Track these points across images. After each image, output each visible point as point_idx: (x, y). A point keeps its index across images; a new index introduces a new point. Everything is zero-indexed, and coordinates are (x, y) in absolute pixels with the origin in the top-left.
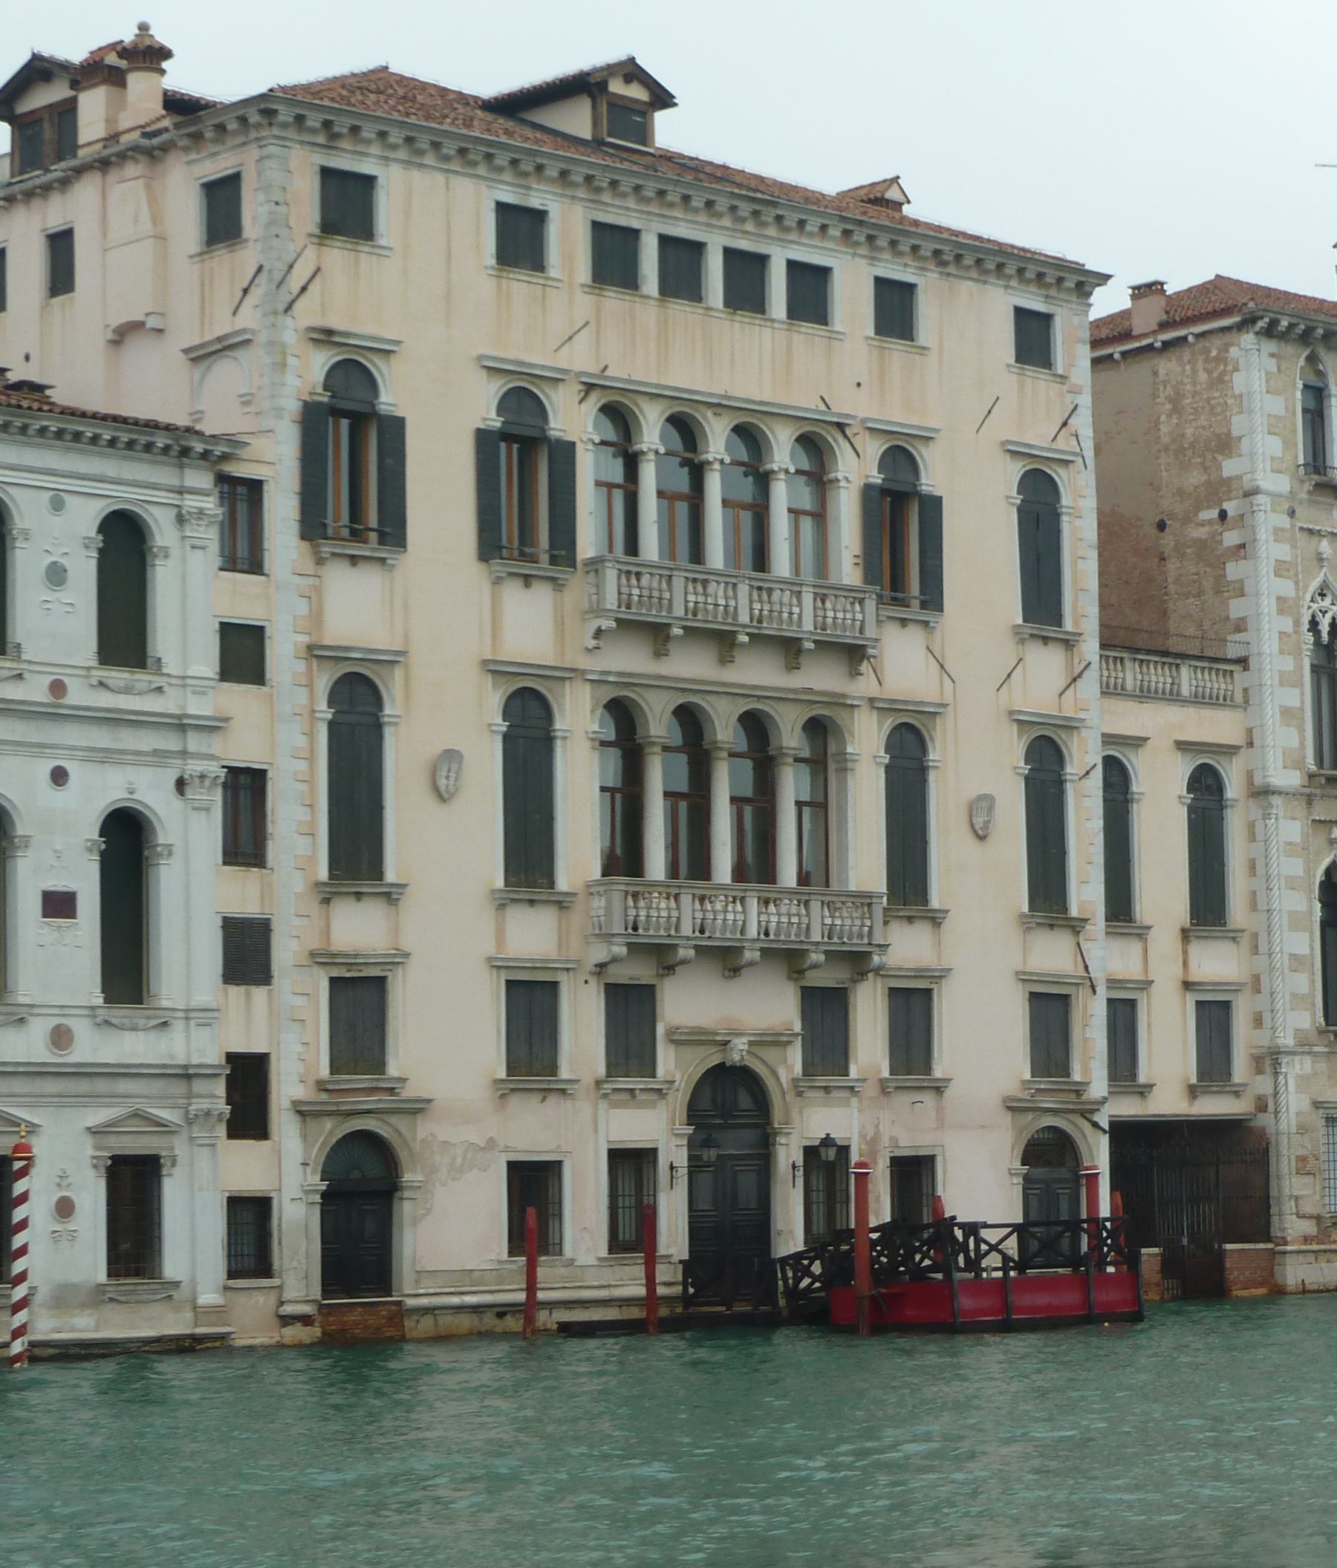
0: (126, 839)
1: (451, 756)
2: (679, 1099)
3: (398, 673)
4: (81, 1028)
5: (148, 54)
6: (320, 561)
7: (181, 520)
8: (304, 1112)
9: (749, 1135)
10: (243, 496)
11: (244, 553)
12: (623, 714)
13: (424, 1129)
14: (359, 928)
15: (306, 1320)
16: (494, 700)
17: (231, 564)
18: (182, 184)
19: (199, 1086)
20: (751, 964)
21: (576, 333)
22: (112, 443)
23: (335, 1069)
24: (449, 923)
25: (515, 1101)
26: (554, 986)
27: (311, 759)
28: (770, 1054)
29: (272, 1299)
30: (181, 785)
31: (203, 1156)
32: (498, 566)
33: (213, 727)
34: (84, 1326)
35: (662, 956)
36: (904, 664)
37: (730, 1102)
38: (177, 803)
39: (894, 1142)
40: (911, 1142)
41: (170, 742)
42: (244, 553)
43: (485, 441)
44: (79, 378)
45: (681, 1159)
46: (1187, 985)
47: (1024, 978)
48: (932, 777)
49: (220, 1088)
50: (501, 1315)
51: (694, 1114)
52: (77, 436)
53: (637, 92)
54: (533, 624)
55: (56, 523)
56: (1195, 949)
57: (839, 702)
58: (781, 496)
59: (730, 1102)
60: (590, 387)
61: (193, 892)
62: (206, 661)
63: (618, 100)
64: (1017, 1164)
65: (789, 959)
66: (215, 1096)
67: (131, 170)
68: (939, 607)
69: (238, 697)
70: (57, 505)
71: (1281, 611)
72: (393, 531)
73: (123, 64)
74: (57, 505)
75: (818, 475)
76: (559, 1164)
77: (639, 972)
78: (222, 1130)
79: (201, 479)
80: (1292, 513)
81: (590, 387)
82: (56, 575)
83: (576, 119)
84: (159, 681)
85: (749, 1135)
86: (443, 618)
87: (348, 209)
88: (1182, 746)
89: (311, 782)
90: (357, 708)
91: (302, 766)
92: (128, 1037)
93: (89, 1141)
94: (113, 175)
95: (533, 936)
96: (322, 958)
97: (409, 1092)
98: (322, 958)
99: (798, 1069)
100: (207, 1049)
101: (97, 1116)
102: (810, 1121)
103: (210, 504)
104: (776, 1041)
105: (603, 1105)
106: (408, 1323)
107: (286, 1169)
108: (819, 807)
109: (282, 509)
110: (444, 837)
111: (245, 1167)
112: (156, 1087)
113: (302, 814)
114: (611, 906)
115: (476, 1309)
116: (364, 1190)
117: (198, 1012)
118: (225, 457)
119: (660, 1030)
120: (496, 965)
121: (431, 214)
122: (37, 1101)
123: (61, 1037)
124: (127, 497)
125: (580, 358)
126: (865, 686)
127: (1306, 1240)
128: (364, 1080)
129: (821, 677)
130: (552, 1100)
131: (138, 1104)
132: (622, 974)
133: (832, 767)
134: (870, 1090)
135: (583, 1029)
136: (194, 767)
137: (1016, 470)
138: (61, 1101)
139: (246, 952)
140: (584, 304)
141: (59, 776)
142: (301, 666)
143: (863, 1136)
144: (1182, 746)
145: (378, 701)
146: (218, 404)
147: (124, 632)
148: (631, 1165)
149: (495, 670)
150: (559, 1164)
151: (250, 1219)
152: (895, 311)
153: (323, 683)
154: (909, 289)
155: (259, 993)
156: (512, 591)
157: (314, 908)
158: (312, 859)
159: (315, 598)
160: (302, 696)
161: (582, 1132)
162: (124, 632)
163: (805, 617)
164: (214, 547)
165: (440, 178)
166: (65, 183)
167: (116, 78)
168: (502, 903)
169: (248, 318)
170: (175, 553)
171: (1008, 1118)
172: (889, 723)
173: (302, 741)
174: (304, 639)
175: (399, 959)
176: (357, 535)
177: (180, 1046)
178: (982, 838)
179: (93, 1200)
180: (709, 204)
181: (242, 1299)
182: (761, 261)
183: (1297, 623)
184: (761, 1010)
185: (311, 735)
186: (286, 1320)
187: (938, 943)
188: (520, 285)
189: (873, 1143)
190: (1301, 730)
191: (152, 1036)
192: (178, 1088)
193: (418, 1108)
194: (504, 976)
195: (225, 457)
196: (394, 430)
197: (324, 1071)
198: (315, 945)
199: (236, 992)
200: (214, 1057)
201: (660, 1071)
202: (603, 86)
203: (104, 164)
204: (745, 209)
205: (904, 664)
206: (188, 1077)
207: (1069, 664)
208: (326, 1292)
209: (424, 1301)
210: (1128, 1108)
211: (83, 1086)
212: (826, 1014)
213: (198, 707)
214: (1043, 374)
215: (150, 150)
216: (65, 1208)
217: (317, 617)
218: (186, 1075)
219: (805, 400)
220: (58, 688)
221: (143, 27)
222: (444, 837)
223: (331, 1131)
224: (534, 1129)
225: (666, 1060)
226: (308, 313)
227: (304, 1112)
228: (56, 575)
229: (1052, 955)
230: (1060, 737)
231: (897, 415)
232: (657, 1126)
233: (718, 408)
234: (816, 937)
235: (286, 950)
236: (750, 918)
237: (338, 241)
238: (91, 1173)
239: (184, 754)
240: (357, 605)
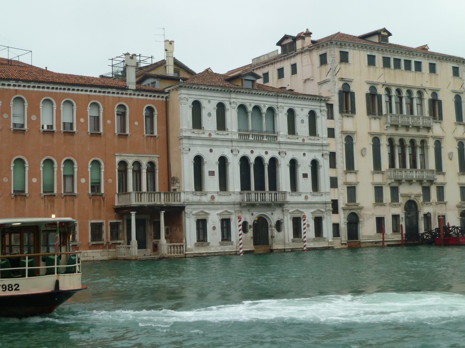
0: (315, 164)
1: (365, 149)
2: (403, 206)
3: (355, 135)
4: (309, 196)
5: (308, 34)
6: (342, 117)
7: (321, 111)
8: (344, 209)
9: (414, 212)
10: (330, 107)
11: (331, 116)
12: (391, 141)
14: (351, 178)
15: (345, 244)
16: (370, 139)
17: (328, 118)
18: (316, 56)
19: (327, 205)
20: (414, 183)
21: (382, 76)
22: (310, 99)
23: (348, 202)
24: (365, 177)
25: (377, 207)
26: (382, 187)
27: (342, 150)
28: (417, 198)
29: (340, 241)
30: (323, 155)
31: (329, 216)
32: (371, 116)
33: (327, 145)
34: (312, 245)
35: (399, 181)
36: (437, 130)
37: (411, 206)
38: (322, 158)
39: (438, 213)
40: (441, 212)
41: (320, 148)
42: (331, 116)
43: (367, 95)
44: (299, 88)
45: (404, 216)
47: (459, 184)
48: (442, 149)
49: (331, 205)
50: (376, 243)
51: (406, 209)
52: (305, 98)
53: (386, 34)
54: (376, 126)
55: (302, 112)
57: (427, 137)
58: (415, 102)
59: (411, 206)
60: (383, 85)
61: (325, 173)
62: (325, 135)
63: (382, 35)
64: (459, 217)
65: (420, 182)
66: (330, 207)
67: (307, 53)
68: (442, 120)
69: (331, 140)
70: (302, 110)
72: (353, 111)
73: (304, 36)
74: (302, 110)
75: (421, 98)
76: (384, 217)
77: (396, 185)
78: (331, 212)
79: (324, 104)
81: (383, 85)
82: (302, 121)
83: (376, 39)
84: (319, 138)
85: (414, 212)
86: (362, 125)
87: (344, 58)
89: (342, 154)
90: (349, 141)
91: (341, 151)
92: (316, 197)
93: (311, 214)
94: (303, 54)
95: (378, 179)
96: (345, 183)
97: (360, 206)
98: (345, 183)
99: (422, 201)
100: (328, 199)
101: (312, 210)
102: (425, 210)
103: (325, 108)
104: (418, 196)
105: (391, 207)
106: (361, 245)
107: (341, 219)
108: (423, 155)
109: (336, 109)
110: (364, 163)
111: (335, 218)
112: (321, 205)
113: (341, 159)
114: (391, 173)
115: (372, 242)
116: (354, 222)
118: (327, 100)
119: (399, 194)
120: (373, 184)
121: (358, 57)
122: (303, 208)
123: (306, 197)
124: (312, 108)
125: (382, 80)
126: (430, 134)
128: (353, 204)
129: (423, 133)
130: (383, 207)
131: (318, 208)
132: (393, 185)
133: (425, 148)
134: (434, 204)
135: (387, 195)
136: (325, 152)
137: (454, 95)
138: (307, 208)
139: (334, 183)
140: (382, 70)
141: (304, 154)
142: (340, 135)
143: (433, 212)
145: (352, 140)
146: (324, 91)
147: (313, 131)
148: (395, 217)
149: (370, 134)
150: (384, 217)
151: (336, 227)
152: (432, 68)
153: (344, 137)
154: (434, 64)
155: (336, 189)
156: (373, 120)
157: (344, 175)
158: (343, 167)
160: (340, 140)
161: (388, 212)
162: (313, 131)
163: (421, 122)
164: (326, 115)
165: (358, 51)
166: (294, 56)
167: (303, 38)
168: (373, 173)
169: (329, 77)
170: (320, 117)
171: (457, 209)
172: (435, 140)
173: (341, 147)
174: (340, 130)
175: (357, 183)
176: (347, 112)
178: (451, 159)
180: (401, 52)
181: (335, 240)
182: (410, 61)
185: (342, 146)
186: (342, 244)
187: (444, 178)
188: (372, 68)
189: (435, 214)
191: (320, 197)
192: (324, 205)
193: (361, 208)
194: (374, 186)
195: (327, 100)
196: (353, 94)
197: (347, 202)
198: (344, 181)
199: (332, 189)
200: (329, 200)
201: (400, 201)
202: (380, 33)
203: (302, 53)
204: (407, 53)
205: (437, 130)
206: (326, 204)
208: (348, 239)
209: (364, 241)
211: (310, 205)
212: (426, 190)
213: (325, 142)
214: (457, 78)
215: (310, 50)
217: (342, 126)
218: (325, 203)
219: (418, 85)
220: (303, 140)
221: (307, 29)
222: (364, 163)
223: (348, 212)
224: (380, 212)
225: (401, 200)
226: (339, 76)
227: (344, 209)
228: (302, 121)
231: (434, 86)
232: (399, 211)
233: (404, 87)
234: (425, 178)
235: (340, 182)
236: (415, 175)
237: (343, 63)
238: (312, 220)
239: (323, 150)
240: (349, 124)
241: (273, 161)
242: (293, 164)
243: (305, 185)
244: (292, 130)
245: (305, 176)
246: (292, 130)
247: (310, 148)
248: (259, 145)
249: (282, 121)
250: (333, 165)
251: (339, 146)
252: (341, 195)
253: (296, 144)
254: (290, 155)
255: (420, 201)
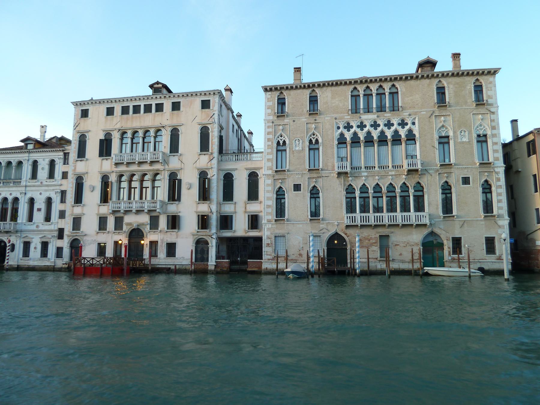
0: (49, 201)
4: (40, 225)
13: (85, 238)
14: (78, 210)
15: (66, 264)
17: (64, 164)
33: (61, 185)
36: (174, 163)
37: (136, 234)
39: (167, 240)
43: (101, 141)
46: (245, 212)
56: (248, 206)
57: (158, 170)
59: (136, 234)
61: (57, 207)
66: (56, 234)
69: (64, 181)
71: (268, 141)
74: (44, 160)
79: (62, 153)
80: (273, 122)
86: (94, 167)
88: (247, 169)
103: (62, 157)
107: (65, 244)
110: (92, 197)
116: (76, 247)
117: (56, 223)
123: (37, 226)
124: (53, 158)
125: (118, 126)
127: (269, 260)
135: (111, 223)
137: (199, 127)
139: (62, 214)
141: (41, 194)
144: (247, 169)
147: (51, 175)
152: (176, 106)
153: (75, 177)
155: (63, 220)
156: (105, 161)
159: (75, 167)
162: (51, 175)
172: (169, 173)
173: (71, 186)
177: (52, 227)
179: (39, 247)
183: (272, 143)
184: (145, 219)
185: (73, 185)
186: (63, 264)
187: (177, 207)
189: (162, 241)
190: (272, 162)
197: (71, 230)
207: (210, 157)
210: (227, 234)
211: (40, 232)
216: (35, 248)
220: (41, 183)
222: (92, 197)
224: (103, 238)
225: (125, 228)
229: (204, 208)
230: (207, 171)
231: (175, 122)
235: (67, 214)
240: (81, 167)
241: (16, 200)
242: (32, 201)
243: (39, 217)
244: (34, 176)
245: (39, 210)
246: (34, 176)
247: (46, 188)
248: (6, 189)
249: (27, 169)
250: (63, 201)
251: (71, 185)
252: (67, 225)
253: (34, 186)
254: (29, 195)
255: (146, 229)
